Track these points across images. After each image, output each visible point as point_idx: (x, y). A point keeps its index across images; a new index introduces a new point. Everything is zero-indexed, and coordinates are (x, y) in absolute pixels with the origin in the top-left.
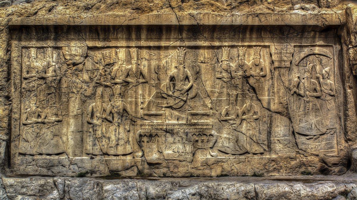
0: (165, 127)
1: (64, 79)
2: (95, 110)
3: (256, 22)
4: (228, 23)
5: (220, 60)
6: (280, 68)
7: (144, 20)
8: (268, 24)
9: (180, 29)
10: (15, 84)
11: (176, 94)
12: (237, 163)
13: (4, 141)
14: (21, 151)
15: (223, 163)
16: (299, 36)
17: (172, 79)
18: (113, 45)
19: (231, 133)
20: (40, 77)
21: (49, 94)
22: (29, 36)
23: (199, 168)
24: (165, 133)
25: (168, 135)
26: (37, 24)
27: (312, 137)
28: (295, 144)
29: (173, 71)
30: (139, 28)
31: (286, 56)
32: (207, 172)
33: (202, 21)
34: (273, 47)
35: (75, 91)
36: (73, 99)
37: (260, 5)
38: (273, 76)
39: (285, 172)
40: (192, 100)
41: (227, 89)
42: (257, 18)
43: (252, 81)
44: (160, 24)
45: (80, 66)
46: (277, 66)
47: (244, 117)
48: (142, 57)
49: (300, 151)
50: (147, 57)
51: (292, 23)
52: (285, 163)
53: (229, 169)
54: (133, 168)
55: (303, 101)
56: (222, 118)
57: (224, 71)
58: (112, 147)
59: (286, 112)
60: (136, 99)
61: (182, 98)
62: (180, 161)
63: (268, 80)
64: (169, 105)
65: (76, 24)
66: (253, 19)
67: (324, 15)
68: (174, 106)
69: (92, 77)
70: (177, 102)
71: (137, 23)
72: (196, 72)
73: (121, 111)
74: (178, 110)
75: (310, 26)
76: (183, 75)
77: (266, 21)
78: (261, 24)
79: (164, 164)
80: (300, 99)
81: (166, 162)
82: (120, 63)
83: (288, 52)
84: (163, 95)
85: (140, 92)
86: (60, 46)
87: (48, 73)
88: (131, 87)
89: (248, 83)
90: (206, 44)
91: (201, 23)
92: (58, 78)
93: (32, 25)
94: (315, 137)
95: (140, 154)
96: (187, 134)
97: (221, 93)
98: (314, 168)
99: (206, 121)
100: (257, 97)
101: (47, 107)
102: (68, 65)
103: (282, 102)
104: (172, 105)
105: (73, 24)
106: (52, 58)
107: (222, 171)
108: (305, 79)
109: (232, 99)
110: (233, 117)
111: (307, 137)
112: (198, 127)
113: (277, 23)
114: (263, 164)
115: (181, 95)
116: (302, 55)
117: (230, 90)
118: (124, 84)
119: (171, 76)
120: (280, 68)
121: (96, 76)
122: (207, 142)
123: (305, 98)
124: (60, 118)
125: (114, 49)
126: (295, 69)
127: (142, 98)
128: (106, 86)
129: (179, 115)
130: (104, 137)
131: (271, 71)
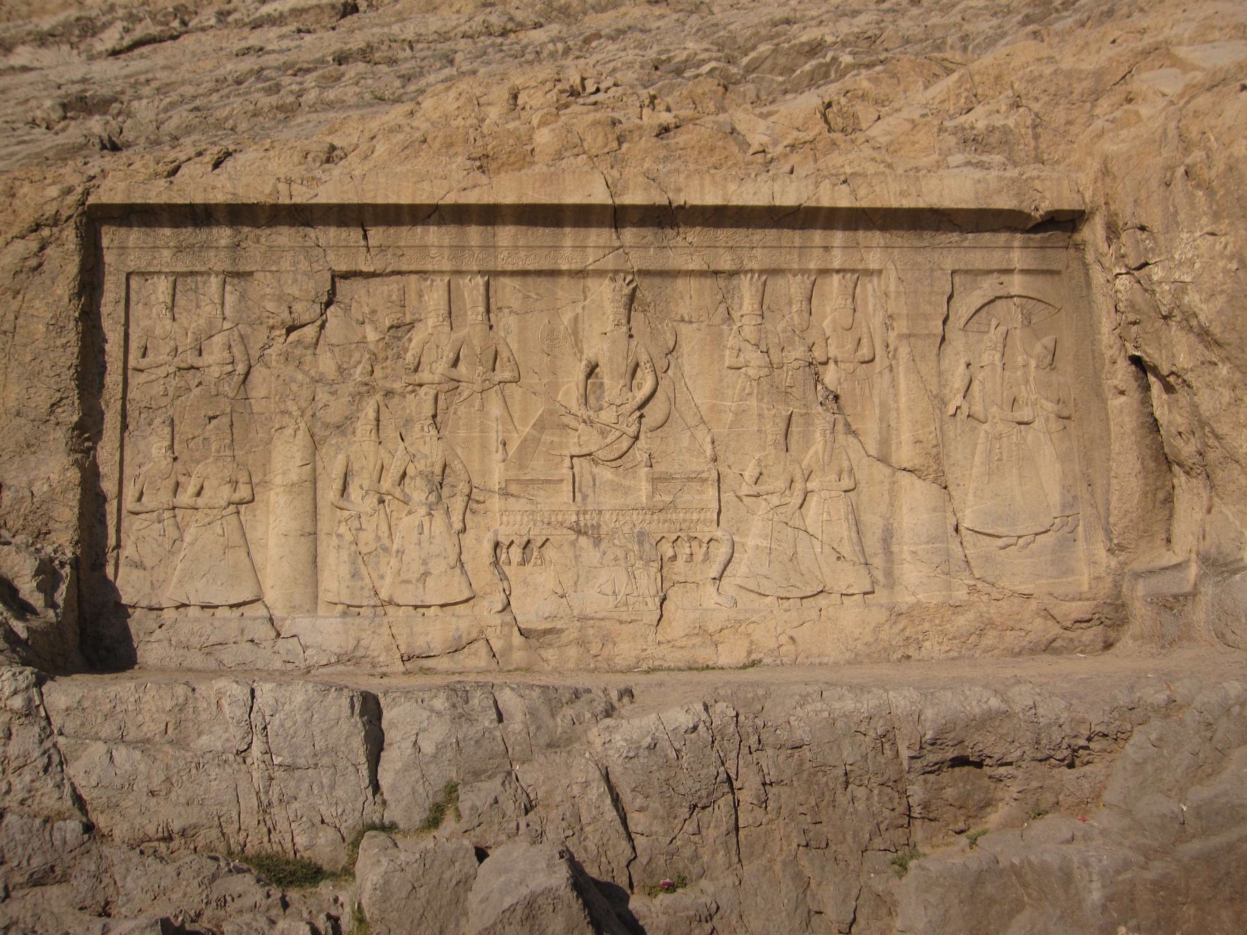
1: (258, 374)
2: (356, 467)
5: (736, 315)
6: (915, 336)
7: (506, 190)
8: (879, 205)
12: (796, 624)
15: (752, 626)
16: (966, 244)
17: (592, 370)
18: (412, 268)
19: (775, 534)
20: (183, 365)
21: (211, 419)
22: (150, 240)
23: (678, 644)
24: (574, 537)
25: (583, 540)
26: (174, 201)
27: (1013, 540)
28: (964, 565)
29: (597, 347)
30: (490, 215)
31: (930, 302)
32: (705, 655)
33: (682, 195)
34: (893, 275)
35: (293, 408)
36: (289, 431)
37: (850, 152)
38: (893, 363)
39: (937, 647)
40: (655, 434)
41: (760, 400)
43: (830, 376)
44: (556, 202)
45: (310, 332)
46: (905, 331)
47: (810, 486)
48: (499, 305)
49: (980, 585)
50: (516, 305)
51: (947, 203)
52: (937, 622)
53: (773, 644)
54: (472, 646)
55: (982, 434)
56: (745, 490)
57: (749, 347)
58: (408, 582)
59: (935, 467)
60: (482, 431)
62: (621, 622)
63: (880, 373)
64: (585, 451)
65: (297, 200)
66: (833, 191)
67: (1037, 182)
68: (601, 454)
69: (345, 366)
70: (608, 441)
74: (614, 464)
75: (999, 213)
77: (871, 197)
80: (974, 429)
81: (579, 624)
82: (430, 322)
83: (936, 289)
84: (566, 420)
85: (495, 409)
86: (248, 269)
87: (211, 353)
88: (465, 395)
89: (818, 380)
91: (679, 200)
92: (241, 368)
93: (160, 205)
94: (1021, 541)
95: (498, 601)
96: (641, 537)
97: (740, 413)
98: (1023, 634)
99: (697, 497)
100: (847, 425)
101: (206, 458)
103: (921, 438)
104: (593, 449)
105: (287, 201)
106: (223, 304)
107: (750, 653)
108: (987, 369)
109: (773, 430)
110: (781, 484)
111: (1001, 542)
112: (674, 516)
114: (874, 624)
116: (977, 299)
117: (768, 403)
118: (446, 387)
120: (915, 336)
121: (359, 362)
122: (704, 561)
123: (986, 426)
124: (243, 492)
125: (413, 277)
126: (957, 340)
127: (500, 427)
128: (389, 393)
129: (616, 479)
130: (386, 550)
131: (887, 346)
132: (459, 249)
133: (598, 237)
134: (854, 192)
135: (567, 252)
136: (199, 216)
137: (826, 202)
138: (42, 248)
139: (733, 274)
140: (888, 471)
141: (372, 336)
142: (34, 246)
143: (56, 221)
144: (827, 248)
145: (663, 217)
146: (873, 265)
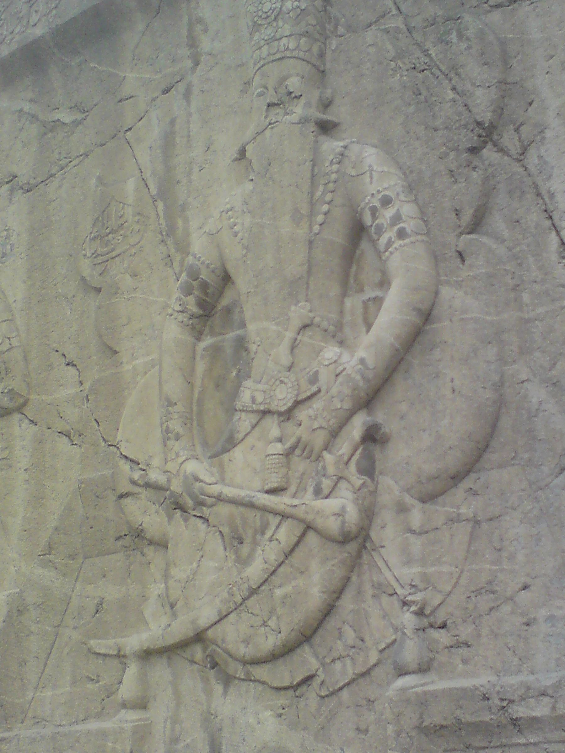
11: (247, 471)
17: (211, 302)
29: (222, 215)
61: (308, 504)
70: (255, 571)
72: (467, 139)
76: (312, 214)
104: (206, 615)
115: (300, 465)
119: (194, 274)
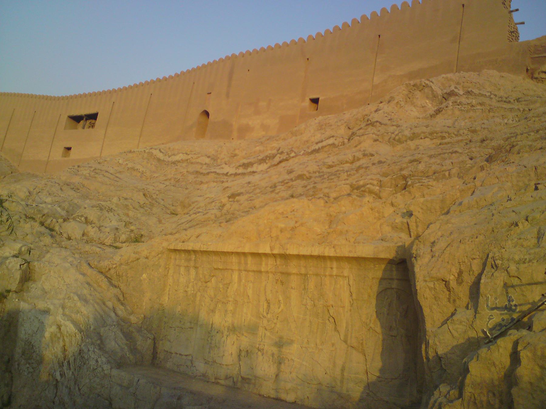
0: (258, 346)
3: (332, 254)
4: (308, 253)
9: (274, 256)
10: (169, 294)
13: (150, 339)
14: (166, 349)
16: (376, 269)
25: (260, 353)
30: (244, 254)
35: (203, 304)
42: (333, 250)
51: (364, 256)
63: (347, 312)
68: (267, 327)
71: (243, 251)
73: (231, 326)
78: (336, 255)
79: (253, 381)
85: (245, 310)
90: (294, 271)
92: (195, 292)
102: (202, 282)
113: (351, 255)
132: (240, 263)
133: (271, 261)
134: (335, 251)
135: (264, 265)
136: (188, 252)
137: (326, 254)
138: (159, 259)
139: (306, 275)
140: (346, 346)
141: (221, 286)
142: (157, 259)
143: (162, 253)
144: (332, 268)
145: (285, 257)
146: (346, 274)
